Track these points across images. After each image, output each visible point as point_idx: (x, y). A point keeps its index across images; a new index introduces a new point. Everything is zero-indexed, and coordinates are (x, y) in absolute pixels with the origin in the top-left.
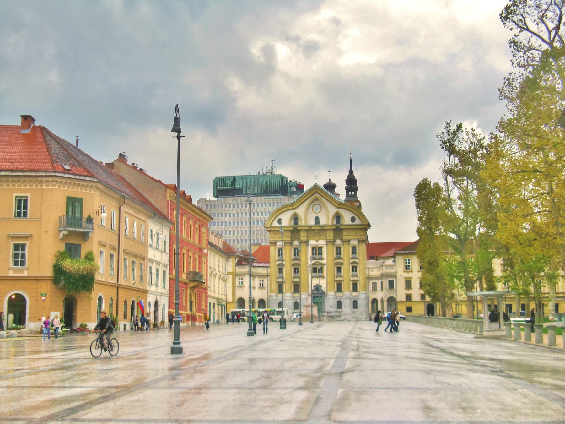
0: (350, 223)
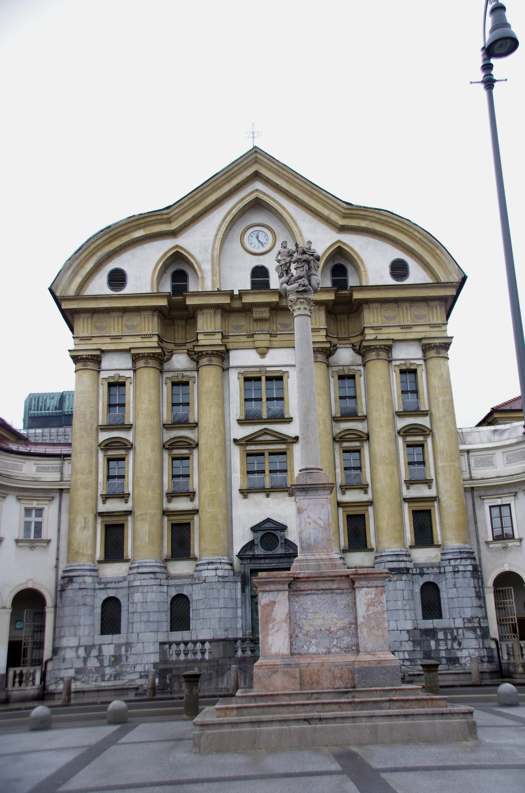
0: (391, 281)
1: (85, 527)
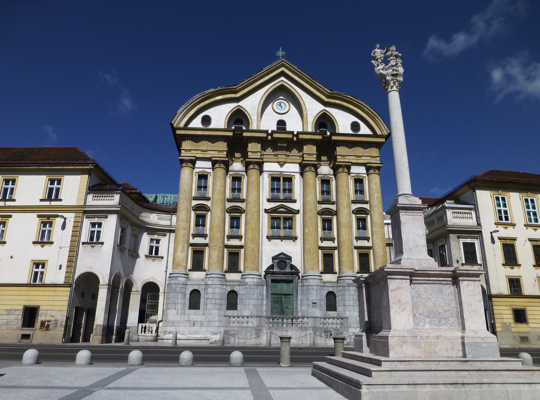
0: (351, 132)
1: (182, 251)
